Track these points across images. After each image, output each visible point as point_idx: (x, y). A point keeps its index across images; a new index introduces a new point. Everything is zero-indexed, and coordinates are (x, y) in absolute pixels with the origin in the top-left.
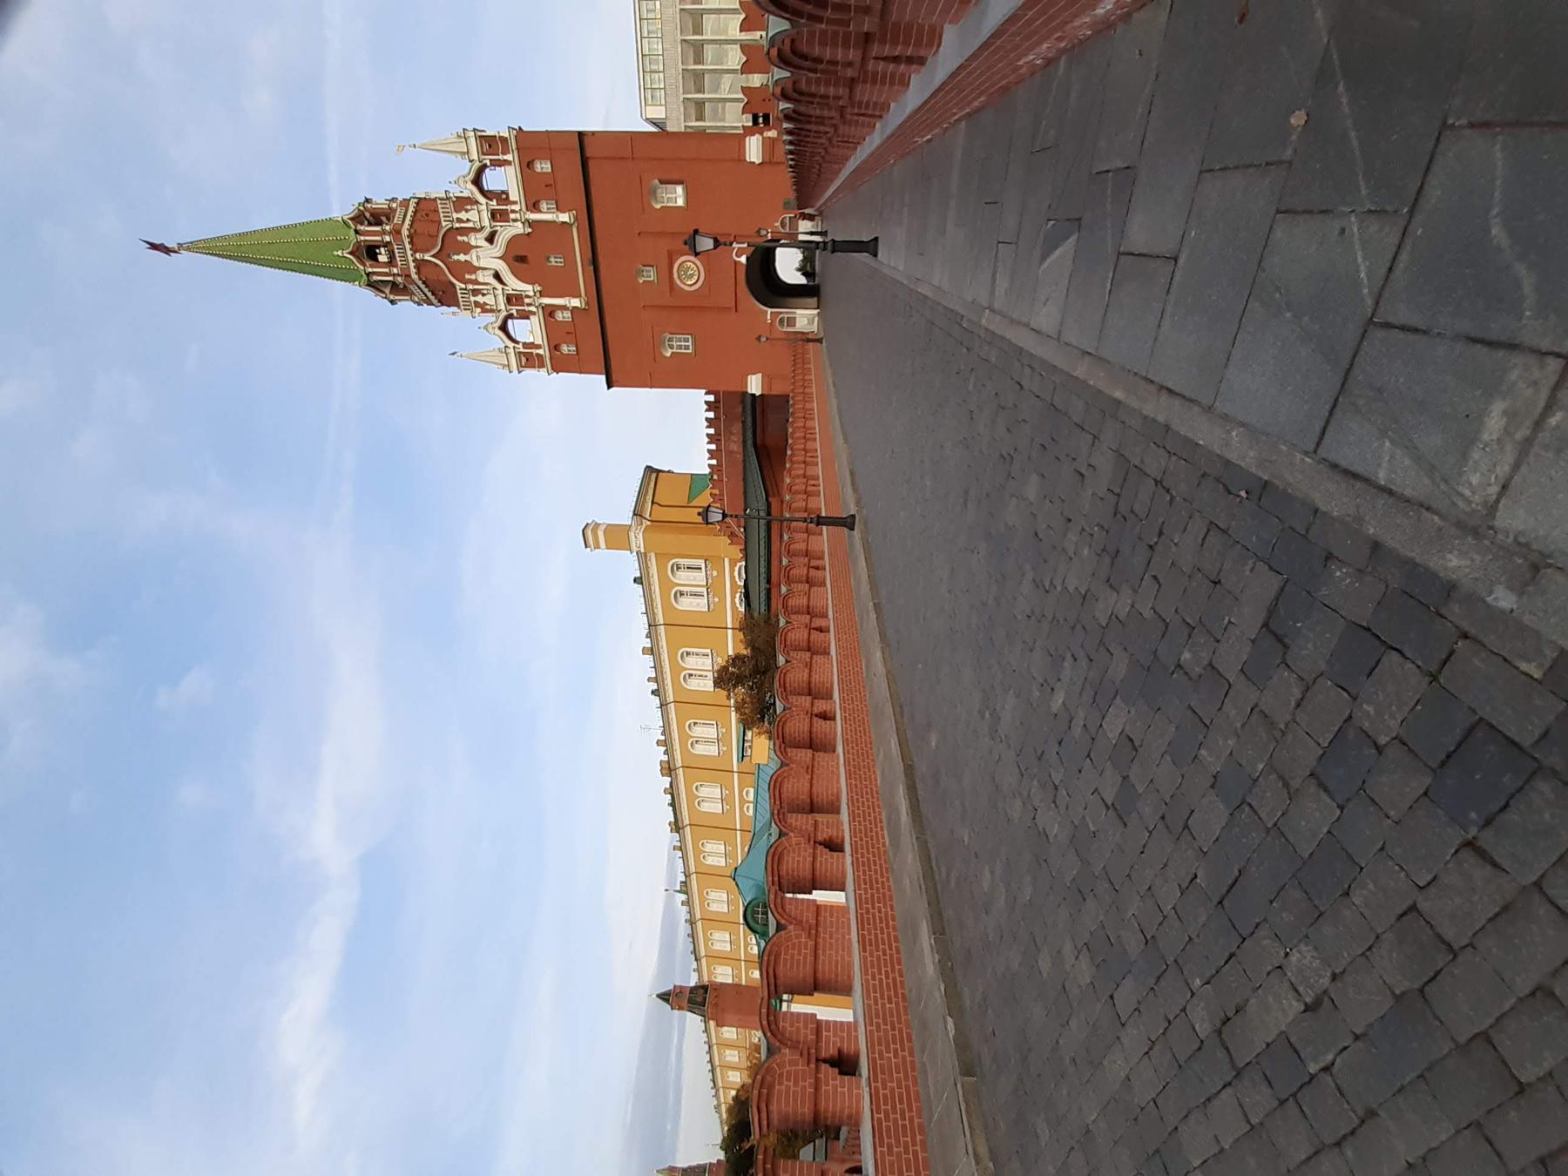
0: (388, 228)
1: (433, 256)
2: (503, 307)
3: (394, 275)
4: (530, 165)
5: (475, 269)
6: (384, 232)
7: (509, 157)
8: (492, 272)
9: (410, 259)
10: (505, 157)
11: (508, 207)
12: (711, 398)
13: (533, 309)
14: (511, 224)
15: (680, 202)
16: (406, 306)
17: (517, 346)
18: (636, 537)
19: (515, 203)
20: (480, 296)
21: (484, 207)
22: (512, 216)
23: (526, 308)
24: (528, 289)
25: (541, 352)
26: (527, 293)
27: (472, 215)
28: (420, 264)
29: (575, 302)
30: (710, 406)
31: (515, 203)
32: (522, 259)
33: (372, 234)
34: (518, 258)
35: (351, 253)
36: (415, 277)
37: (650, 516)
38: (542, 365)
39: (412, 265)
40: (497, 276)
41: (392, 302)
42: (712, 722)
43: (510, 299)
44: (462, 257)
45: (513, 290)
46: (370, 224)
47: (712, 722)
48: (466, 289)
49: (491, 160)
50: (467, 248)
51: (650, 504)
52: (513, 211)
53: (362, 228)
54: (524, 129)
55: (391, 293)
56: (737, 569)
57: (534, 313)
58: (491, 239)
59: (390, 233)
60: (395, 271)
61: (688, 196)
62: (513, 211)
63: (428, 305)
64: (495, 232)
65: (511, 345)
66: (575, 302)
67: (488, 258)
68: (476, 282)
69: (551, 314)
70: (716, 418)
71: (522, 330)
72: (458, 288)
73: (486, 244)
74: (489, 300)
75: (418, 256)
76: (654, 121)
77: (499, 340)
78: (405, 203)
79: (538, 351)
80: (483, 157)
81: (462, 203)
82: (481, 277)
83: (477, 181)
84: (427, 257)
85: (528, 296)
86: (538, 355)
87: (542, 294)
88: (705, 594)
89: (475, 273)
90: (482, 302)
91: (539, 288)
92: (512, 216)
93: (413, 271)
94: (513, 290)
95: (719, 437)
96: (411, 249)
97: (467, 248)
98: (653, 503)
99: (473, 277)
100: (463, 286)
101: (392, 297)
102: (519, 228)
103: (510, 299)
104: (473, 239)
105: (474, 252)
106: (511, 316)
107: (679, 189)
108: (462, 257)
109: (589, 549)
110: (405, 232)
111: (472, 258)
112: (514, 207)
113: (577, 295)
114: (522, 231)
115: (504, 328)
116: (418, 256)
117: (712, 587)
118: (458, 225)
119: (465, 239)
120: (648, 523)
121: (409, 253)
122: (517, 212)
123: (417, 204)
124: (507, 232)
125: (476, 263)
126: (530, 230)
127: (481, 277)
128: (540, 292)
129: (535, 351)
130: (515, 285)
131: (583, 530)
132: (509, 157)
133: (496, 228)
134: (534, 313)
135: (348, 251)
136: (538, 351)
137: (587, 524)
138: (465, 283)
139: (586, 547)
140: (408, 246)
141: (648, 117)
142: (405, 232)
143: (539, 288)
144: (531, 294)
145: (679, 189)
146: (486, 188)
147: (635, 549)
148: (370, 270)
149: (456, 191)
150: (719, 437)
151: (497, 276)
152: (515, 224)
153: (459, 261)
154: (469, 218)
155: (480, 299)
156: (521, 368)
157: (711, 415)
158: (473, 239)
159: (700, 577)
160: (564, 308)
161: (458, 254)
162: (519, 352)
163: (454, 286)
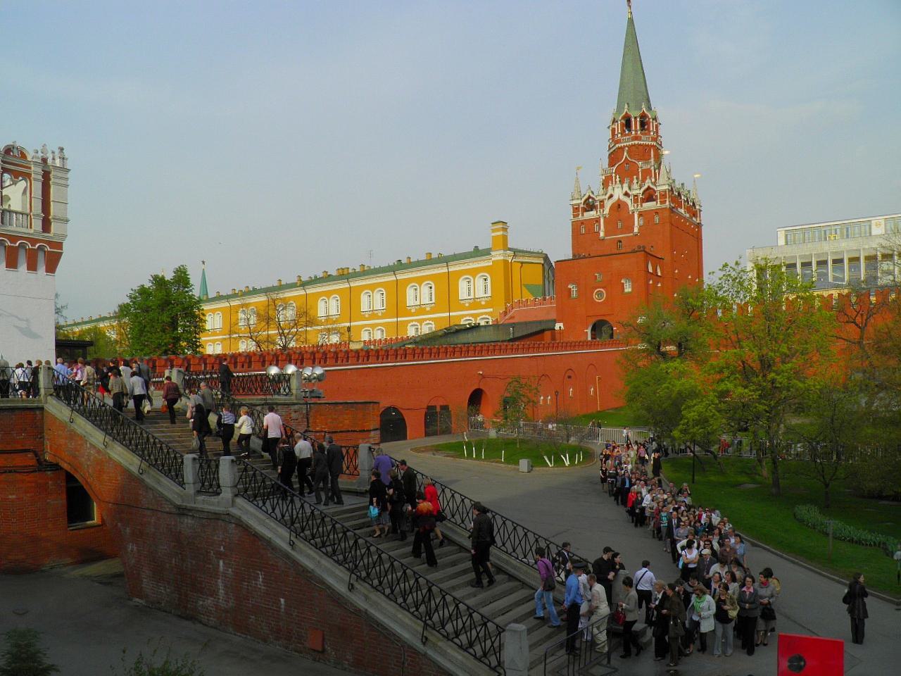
0: (639, 133)
1: (626, 157)
4: (657, 213)
6: (636, 131)
9: (625, 144)
13: (599, 213)
15: (626, 290)
19: (641, 206)
21: (638, 192)
24: (607, 211)
25: (580, 216)
28: (622, 149)
29: (602, 234)
31: (641, 206)
33: (636, 125)
34: (619, 206)
35: (626, 113)
38: (574, 216)
39: (622, 145)
40: (611, 196)
41: (609, 127)
42: (385, 304)
43: (602, 201)
47: (385, 304)
50: (622, 182)
52: (638, 205)
56: (487, 316)
58: (626, 194)
59: (636, 134)
60: (619, 135)
61: (629, 293)
62: (638, 205)
66: (602, 234)
67: (618, 192)
69: (597, 221)
73: (624, 192)
84: (625, 154)
86: (579, 214)
88: (469, 298)
92: (636, 205)
97: (622, 182)
98: (522, 263)
102: (631, 208)
103: (602, 201)
105: (620, 186)
107: (630, 290)
110: (636, 142)
113: (606, 235)
117: (475, 304)
118: (640, 170)
121: (628, 144)
124: (628, 201)
129: (580, 213)
130: (608, 204)
132: (659, 205)
140: (630, 143)
142: (636, 142)
145: (630, 290)
151: (611, 196)
159: (480, 293)
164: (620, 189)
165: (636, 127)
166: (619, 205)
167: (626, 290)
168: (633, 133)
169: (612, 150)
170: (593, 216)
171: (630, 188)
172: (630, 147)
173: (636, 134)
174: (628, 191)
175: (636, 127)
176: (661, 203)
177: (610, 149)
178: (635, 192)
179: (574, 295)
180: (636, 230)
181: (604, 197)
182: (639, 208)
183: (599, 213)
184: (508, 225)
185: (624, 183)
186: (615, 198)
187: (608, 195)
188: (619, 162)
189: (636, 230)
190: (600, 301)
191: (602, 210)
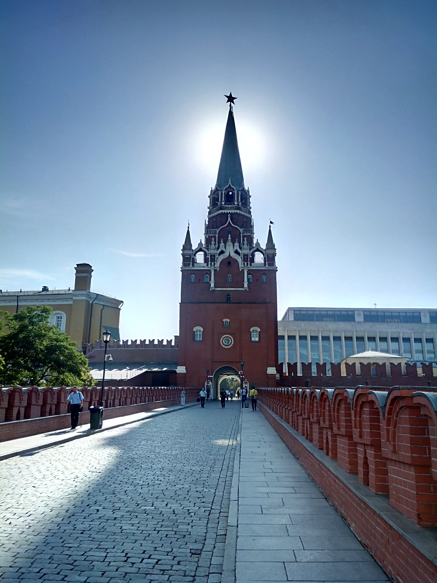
0: (240, 204)
1: (229, 221)
2: (210, 252)
3: (221, 202)
4: (264, 274)
5: (225, 243)
7: (267, 266)
8: (224, 250)
9: (228, 211)
10: (267, 264)
11: (249, 263)
12: (165, 343)
13: (209, 265)
14: (243, 262)
15: (253, 339)
16: (207, 202)
17: (193, 255)
18: (83, 294)
19: (251, 265)
20: (214, 243)
21: (249, 252)
22: (246, 263)
23: (209, 263)
24: (218, 265)
25: (191, 266)
26: (216, 264)
27: (246, 246)
29: (212, 285)
31: (251, 265)
32: (229, 263)
36: (221, 211)
39: (226, 211)
44: (229, 238)
45: (217, 258)
46: (241, 196)
48: (216, 233)
49: (266, 258)
51: (104, 304)
52: (247, 264)
53: (240, 193)
54: (277, 273)
55: (213, 197)
57: (208, 265)
58: (236, 252)
59: (238, 204)
60: (223, 203)
61: (255, 342)
62: (247, 264)
63: (209, 212)
64: (240, 255)
65: (194, 252)
66: (212, 285)
68: (219, 243)
69: (207, 273)
71: (200, 258)
72: (217, 230)
73: (235, 250)
74: (213, 246)
75: (229, 215)
76: (288, 313)
77: (195, 247)
78: (250, 213)
79: (191, 264)
80: (267, 255)
81: (250, 239)
82: (222, 244)
83: (258, 250)
84: (229, 219)
85: (214, 264)
86: (190, 264)
87: (215, 270)
89: (223, 243)
90: (212, 243)
91: (218, 269)
92: (246, 263)
93: (223, 211)
94: (217, 258)
95: (143, 346)
96: (232, 212)
97: (233, 242)
98: (104, 305)
99: (222, 241)
100: (217, 233)
101: (211, 197)
102: (241, 265)
104: (237, 244)
105: (231, 244)
106: (205, 255)
107: (257, 339)
108: (229, 238)
109: (76, 266)
110: (238, 211)
111: (229, 243)
112: (249, 264)
113: (215, 287)
114: (240, 266)
115: (201, 250)
116: (229, 215)
118: (241, 235)
119: (237, 241)
120: (91, 302)
121: (231, 211)
122: (247, 265)
123: (250, 218)
124: (239, 259)
125: (227, 244)
126: (241, 270)
127: (222, 244)
128: (217, 270)
131: (88, 264)
132: (267, 266)
133: (241, 255)
134: (208, 265)
135: (231, 185)
136: (191, 264)
138: (218, 234)
139: (77, 265)
140: (233, 211)
141: (289, 311)
142: (238, 211)
143: (218, 269)
144: (216, 266)
145: (257, 339)
146: (256, 253)
148: (223, 192)
149: (255, 242)
150: (143, 346)
151: (222, 252)
152: (243, 264)
153: (228, 237)
154: (245, 245)
155: (213, 242)
156: (183, 255)
157: (156, 342)
158: (237, 244)
160: (210, 280)
161: (231, 237)
162: (190, 256)
163: (217, 228)
164: (231, 247)
165: (238, 199)
166: (229, 263)
167: (253, 339)
168: (236, 203)
169: (212, 215)
170: (204, 267)
171: (240, 248)
172: (232, 214)
173: (238, 204)
174: (239, 250)
175: (238, 199)
176: (269, 265)
177: (210, 213)
178: (246, 252)
179: (199, 338)
180: (246, 285)
181: (215, 252)
182: (249, 266)
183: (209, 265)
184: (92, 268)
185: (235, 242)
186: (226, 255)
187: (220, 250)
188: (222, 225)
189: (246, 285)
190: (226, 347)
191: (213, 263)
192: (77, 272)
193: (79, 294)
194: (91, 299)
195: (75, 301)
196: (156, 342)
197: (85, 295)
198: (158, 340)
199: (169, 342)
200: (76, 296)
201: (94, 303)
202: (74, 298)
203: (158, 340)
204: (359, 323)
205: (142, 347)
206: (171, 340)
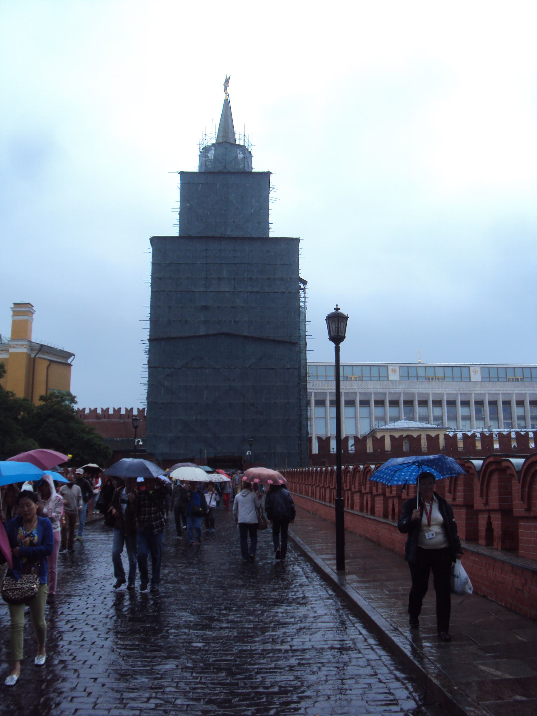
12: (135, 412)
18: (23, 345)
30: (129, 412)
37: (39, 358)
70: (121, 415)
98: (51, 361)
109: (13, 306)
120: (33, 356)
131: (29, 304)
137: (33, 306)
139: (14, 304)
147: (12, 343)
157: (123, 412)
192: (15, 313)
193: (17, 345)
194: (33, 352)
195: (12, 354)
196: (123, 412)
197: (25, 346)
198: (126, 409)
199: (141, 412)
200: (14, 347)
201: (37, 357)
202: (11, 350)
203: (126, 409)
204: (393, 382)
205: (104, 418)
206: (144, 409)
